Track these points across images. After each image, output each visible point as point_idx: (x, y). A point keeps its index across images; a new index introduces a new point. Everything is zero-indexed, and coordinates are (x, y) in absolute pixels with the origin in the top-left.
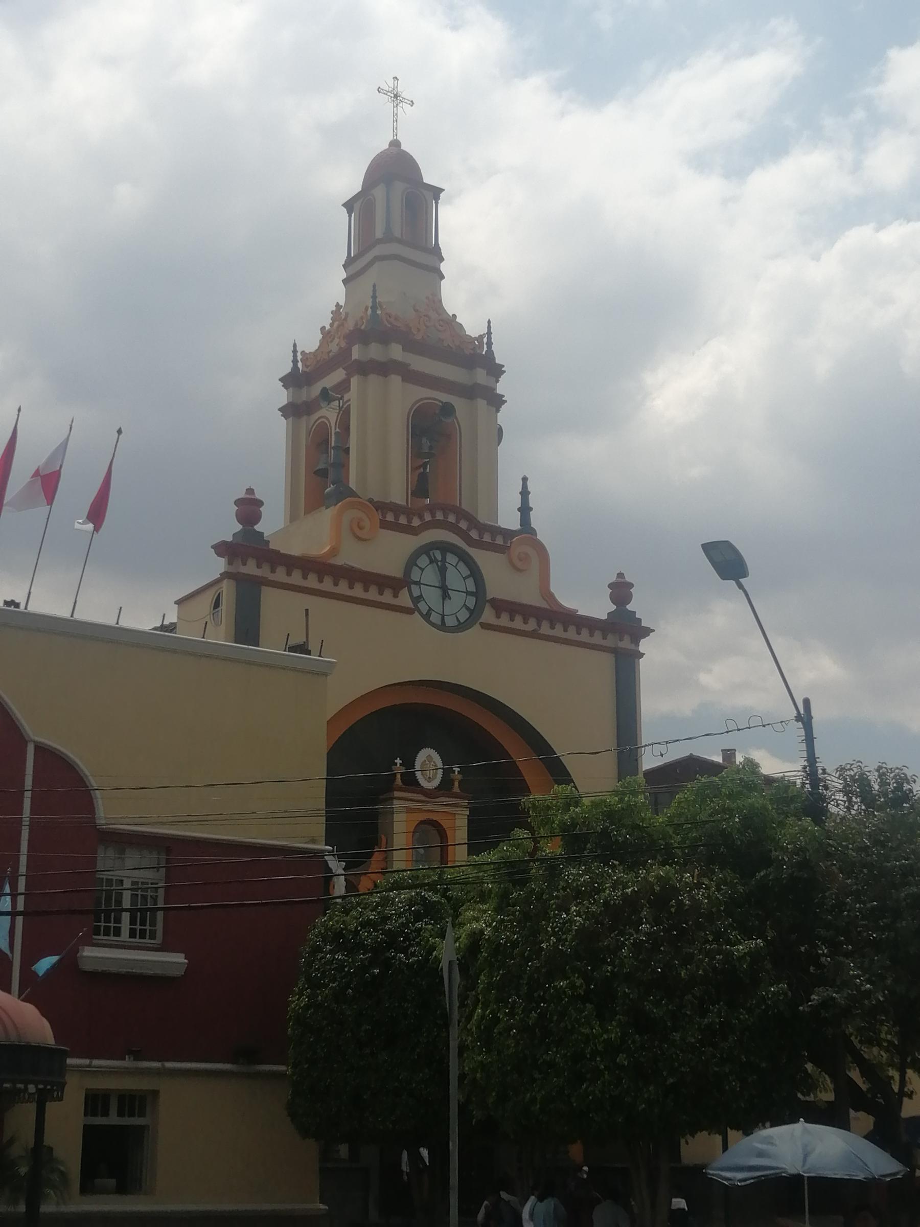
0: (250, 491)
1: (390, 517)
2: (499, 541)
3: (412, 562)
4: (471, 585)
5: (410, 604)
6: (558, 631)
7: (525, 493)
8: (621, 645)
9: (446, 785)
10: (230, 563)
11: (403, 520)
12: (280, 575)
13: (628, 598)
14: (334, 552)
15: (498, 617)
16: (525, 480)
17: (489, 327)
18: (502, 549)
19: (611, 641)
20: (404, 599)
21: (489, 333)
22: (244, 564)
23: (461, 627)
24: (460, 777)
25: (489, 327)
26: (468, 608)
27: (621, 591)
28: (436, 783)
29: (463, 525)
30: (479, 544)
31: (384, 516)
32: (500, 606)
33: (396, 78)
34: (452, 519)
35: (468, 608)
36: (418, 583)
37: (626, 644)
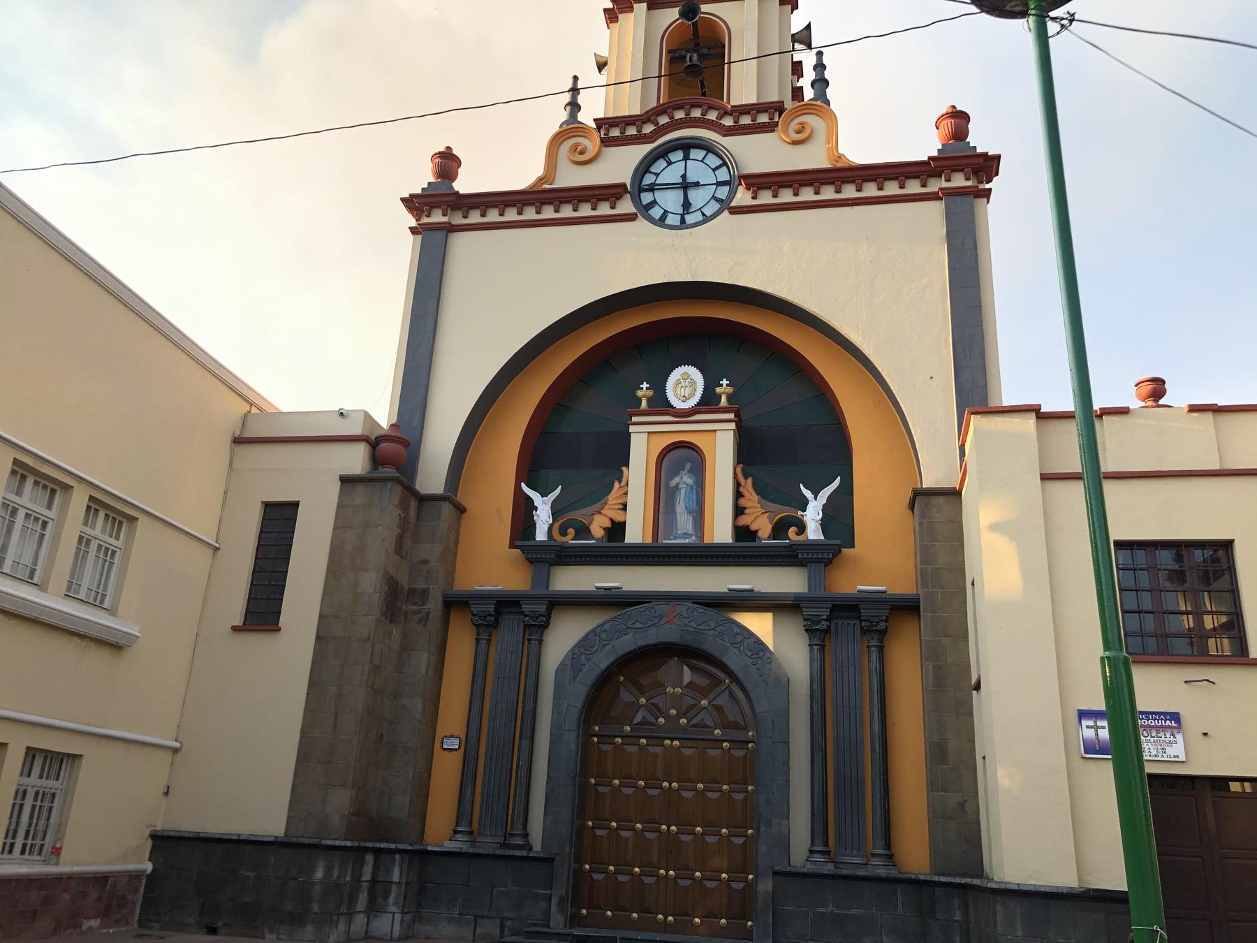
1: (615, 132)
2: (763, 118)
3: (645, 167)
5: (634, 211)
6: (849, 192)
7: (820, 66)
8: (945, 185)
9: (708, 402)
11: (632, 131)
12: (475, 217)
15: (754, 198)
16: (820, 54)
18: (770, 127)
19: (935, 186)
20: (626, 206)
22: (428, 216)
23: (707, 219)
24: (730, 390)
29: (712, 116)
32: (757, 182)
34: (696, 113)
37: (959, 181)
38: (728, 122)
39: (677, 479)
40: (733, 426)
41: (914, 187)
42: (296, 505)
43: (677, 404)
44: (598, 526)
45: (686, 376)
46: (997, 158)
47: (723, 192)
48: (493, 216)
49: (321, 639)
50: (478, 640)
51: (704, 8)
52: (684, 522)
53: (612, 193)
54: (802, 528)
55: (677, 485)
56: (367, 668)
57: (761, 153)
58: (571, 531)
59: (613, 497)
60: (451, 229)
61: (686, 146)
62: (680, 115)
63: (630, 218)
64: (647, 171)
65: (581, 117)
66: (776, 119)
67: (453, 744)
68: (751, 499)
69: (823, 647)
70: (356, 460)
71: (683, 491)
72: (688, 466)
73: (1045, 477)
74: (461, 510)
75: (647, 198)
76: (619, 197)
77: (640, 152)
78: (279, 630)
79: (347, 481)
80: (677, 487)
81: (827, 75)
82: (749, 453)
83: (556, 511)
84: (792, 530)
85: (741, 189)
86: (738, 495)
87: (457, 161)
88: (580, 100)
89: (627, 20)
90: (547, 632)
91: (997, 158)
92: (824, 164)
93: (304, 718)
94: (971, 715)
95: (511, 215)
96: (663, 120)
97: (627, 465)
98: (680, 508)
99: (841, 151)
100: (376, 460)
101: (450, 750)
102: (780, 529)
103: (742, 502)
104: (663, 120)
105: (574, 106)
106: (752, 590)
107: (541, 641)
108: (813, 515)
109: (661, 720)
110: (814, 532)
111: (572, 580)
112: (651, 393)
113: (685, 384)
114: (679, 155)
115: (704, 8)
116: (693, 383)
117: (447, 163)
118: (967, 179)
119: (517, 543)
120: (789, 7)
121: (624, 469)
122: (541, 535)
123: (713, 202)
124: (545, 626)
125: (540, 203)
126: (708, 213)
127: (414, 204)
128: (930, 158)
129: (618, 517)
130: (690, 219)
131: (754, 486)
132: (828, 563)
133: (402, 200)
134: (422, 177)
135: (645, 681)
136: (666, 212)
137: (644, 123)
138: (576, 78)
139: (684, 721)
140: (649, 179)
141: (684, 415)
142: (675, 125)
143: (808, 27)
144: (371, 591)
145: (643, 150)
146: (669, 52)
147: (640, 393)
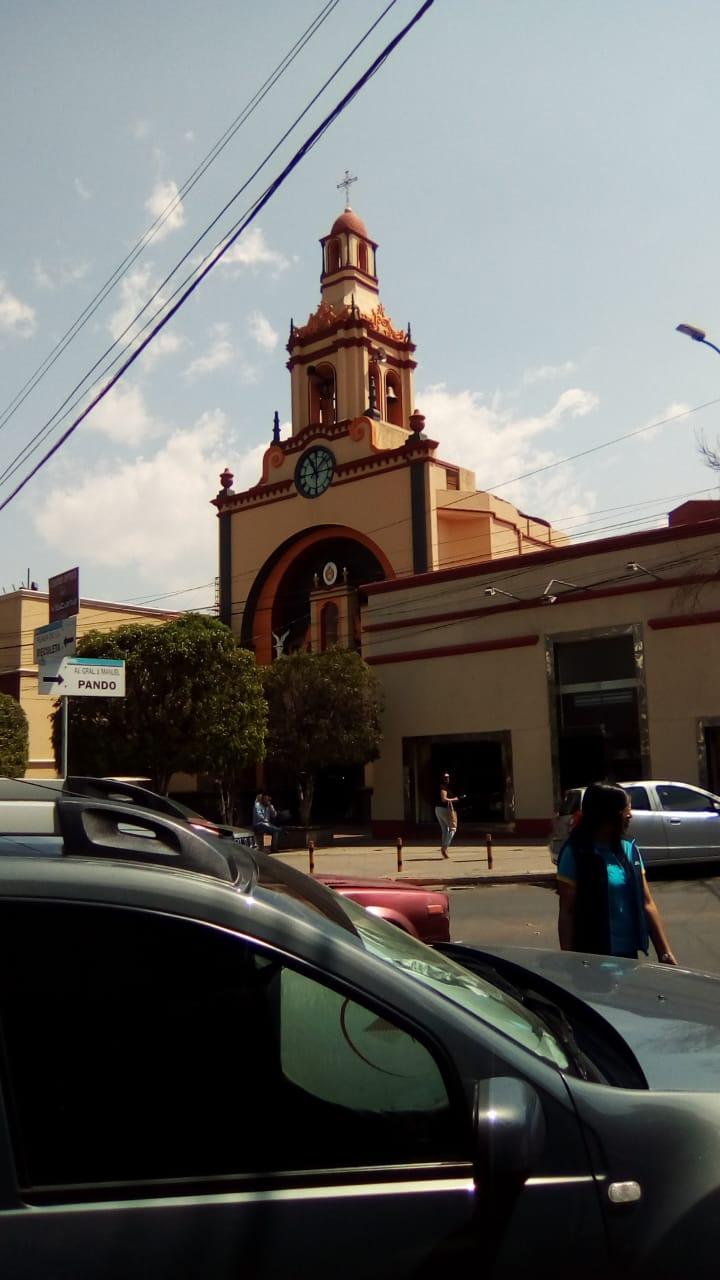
0: (226, 470)
2: (343, 430)
3: (300, 466)
10: (219, 509)
11: (294, 446)
13: (422, 427)
14: (263, 480)
18: (346, 434)
20: (293, 489)
23: (325, 489)
28: (334, 580)
33: (347, 172)
36: (304, 476)
37: (416, 455)
43: (329, 583)
45: (330, 568)
53: (286, 484)
57: (344, 450)
63: (294, 495)
66: (349, 428)
75: (303, 481)
85: (336, 475)
88: (280, 427)
89: (297, 367)
105: (277, 430)
117: (226, 479)
118: (419, 453)
125: (260, 493)
126: (325, 485)
128: (402, 447)
130: (319, 490)
136: (310, 488)
138: (276, 414)
141: (331, 587)
142: (311, 439)
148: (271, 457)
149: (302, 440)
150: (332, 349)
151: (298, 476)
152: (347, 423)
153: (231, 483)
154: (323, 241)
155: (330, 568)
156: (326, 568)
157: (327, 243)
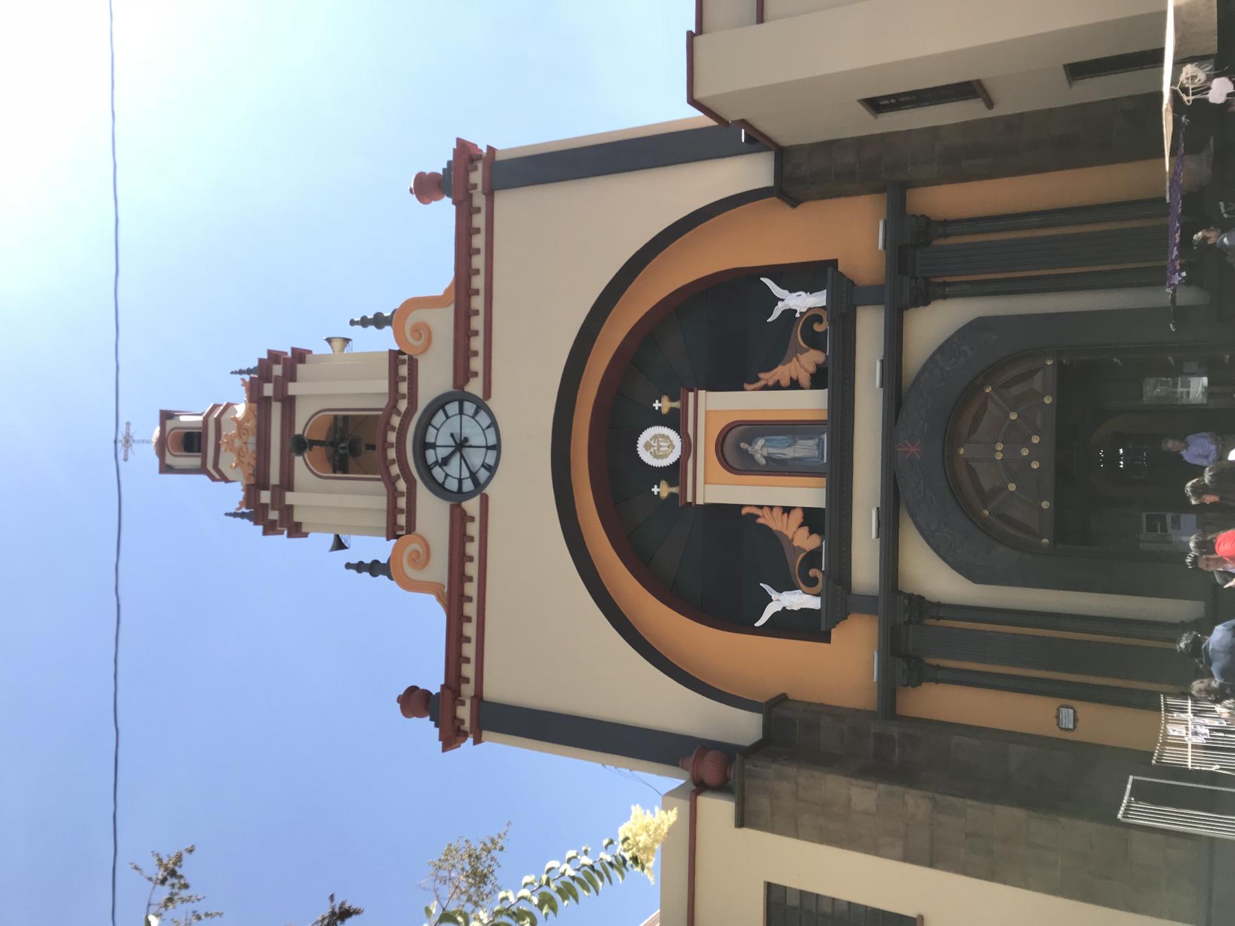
1: (402, 520)
2: (404, 370)
3: (438, 489)
4: (453, 408)
6: (478, 282)
7: (364, 322)
8: (480, 188)
9: (675, 421)
11: (402, 503)
12: (468, 670)
15: (476, 374)
16: (353, 323)
17: (236, 373)
18: (413, 364)
19: (479, 200)
20: (472, 506)
21: (241, 372)
22: (462, 722)
23: (494, 424)
24: (665, 399)
25: (236, 373)
26: (476, 413)
27: (426, 187)
29: (396, 421)
30: (413, 396)
31: (401, 528)
32: (462, 373)
34: (392, 437)
35: (476, 413)
36: (460, 481)
37: (477, 177)
38: (403, 405)
39: (758, 457)
40: (702, 393)
41: (479, 221)
42: (769, 887)
44: (805, 541)
45: (648, 446)
46: (459, 141)
47: (469, 408)
48: (469, 650)
49: (932, 861)
50: (937, 681)
51: (298, 430)
52: (804, 449)
53: (459, 520)
54: (813, 316)
55: (765, 458)
56: (970, 802)
58: (813, 572)
59: (775, 522)
60: (478, 697)
61: (423, 446)
62: (392, 454)
64: (442, 486)
65: (383, 560)
67: (1067, 716)
68: (782, 372)
69: (945, 284)
70: (718, 810)
71: (772, 450)
72: (742, 445)
73: (760, 19)
74: (782, 699)
76: (464, 512)
77: (423, 493)
78: (921, 917)
79: (742, 821)
80: (768, 458)
81: (370, 316)
82: (732, 378)
83: (786, 585)
84: (818, 328)
86: (777, 386)
87: (412, 690)
88: (368, 561)
90: (928, 598)
91: (460, 142)
92: (452, 307)
93: (1035, 890)
94: (1021, 115)
95: (470, 630)
96: (395, 470)
97: (743, 506)
98: (789, 453)
99: (440, 292)
100: (721, 788)
101: (1075, 720)
102: (814, 341)
103: (785, 382)
104: (395, 470)
105: (374, 568)
106: (882, 361)
107: (939, 605)
108: (801, 302)
109: (1035, 465)
110: (818, 300)
111: (865, 569)
112: (664, 484)
113: (656, 446)
114: (431, 456)
115: (298, 430)
116: (655, 437)
117: (414, 701)
118: (476, 169)
119: (823, 628)
120: (308, 357)
121: (744, 511)
122: (814, 603)
123: (477, 418)
124: (921, 599)
125: (461, 601)
127: (451, 737)
128: (454, 203)
129: (797, 517)
130: (492, 441)
131: (769, 368)
132: (851, 283)
133: (444, 750)
134: (426, 729)
135: (986, 484)
137: (396, 489)
138: (348, 566)
139: (1036, 440)
140: (452, 485)
141: (688, 447)
143: (329, 340)
144: (875, 794)
145: (422, 490)
146: (335, 472)
147: (664, 495)
148: (411, 573)
149: (397, 477)
150: (289, 403)
151: (456, 498)
152: (395, 357)
153: (427, 693)
154: (165, 469)
155: (648, 446)
156: (646, 456)
157: (170, 460)
